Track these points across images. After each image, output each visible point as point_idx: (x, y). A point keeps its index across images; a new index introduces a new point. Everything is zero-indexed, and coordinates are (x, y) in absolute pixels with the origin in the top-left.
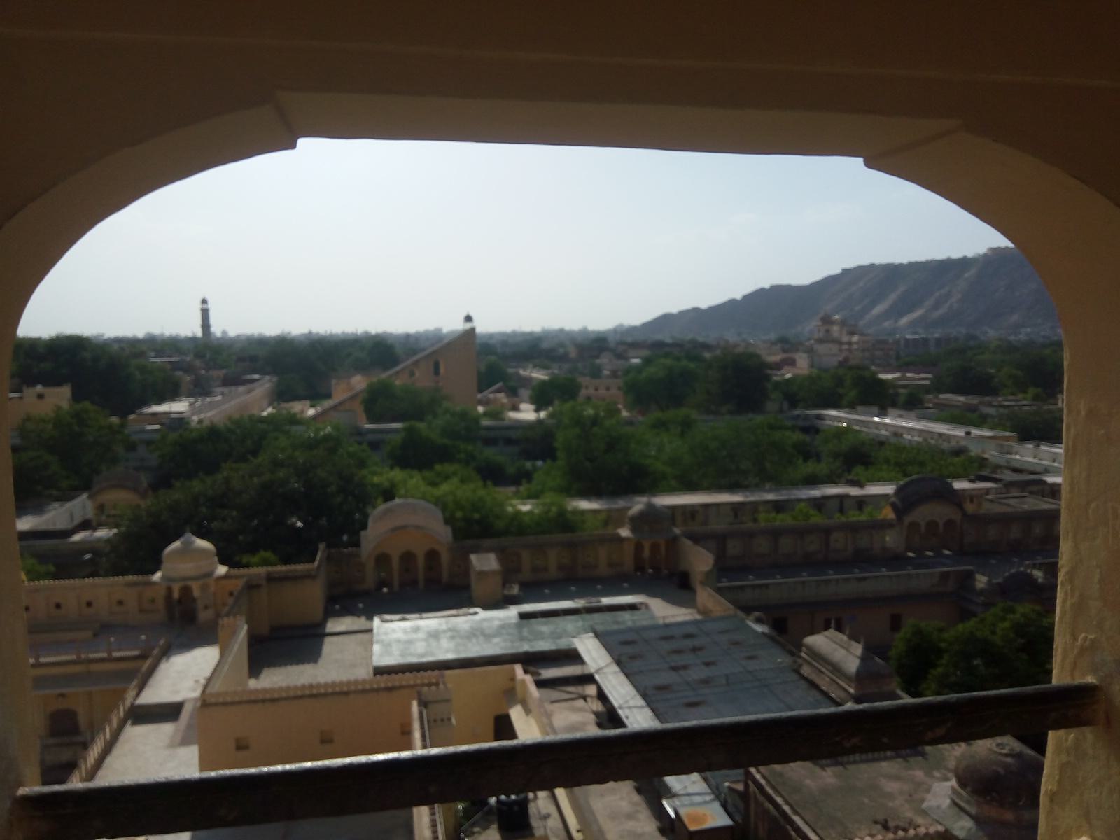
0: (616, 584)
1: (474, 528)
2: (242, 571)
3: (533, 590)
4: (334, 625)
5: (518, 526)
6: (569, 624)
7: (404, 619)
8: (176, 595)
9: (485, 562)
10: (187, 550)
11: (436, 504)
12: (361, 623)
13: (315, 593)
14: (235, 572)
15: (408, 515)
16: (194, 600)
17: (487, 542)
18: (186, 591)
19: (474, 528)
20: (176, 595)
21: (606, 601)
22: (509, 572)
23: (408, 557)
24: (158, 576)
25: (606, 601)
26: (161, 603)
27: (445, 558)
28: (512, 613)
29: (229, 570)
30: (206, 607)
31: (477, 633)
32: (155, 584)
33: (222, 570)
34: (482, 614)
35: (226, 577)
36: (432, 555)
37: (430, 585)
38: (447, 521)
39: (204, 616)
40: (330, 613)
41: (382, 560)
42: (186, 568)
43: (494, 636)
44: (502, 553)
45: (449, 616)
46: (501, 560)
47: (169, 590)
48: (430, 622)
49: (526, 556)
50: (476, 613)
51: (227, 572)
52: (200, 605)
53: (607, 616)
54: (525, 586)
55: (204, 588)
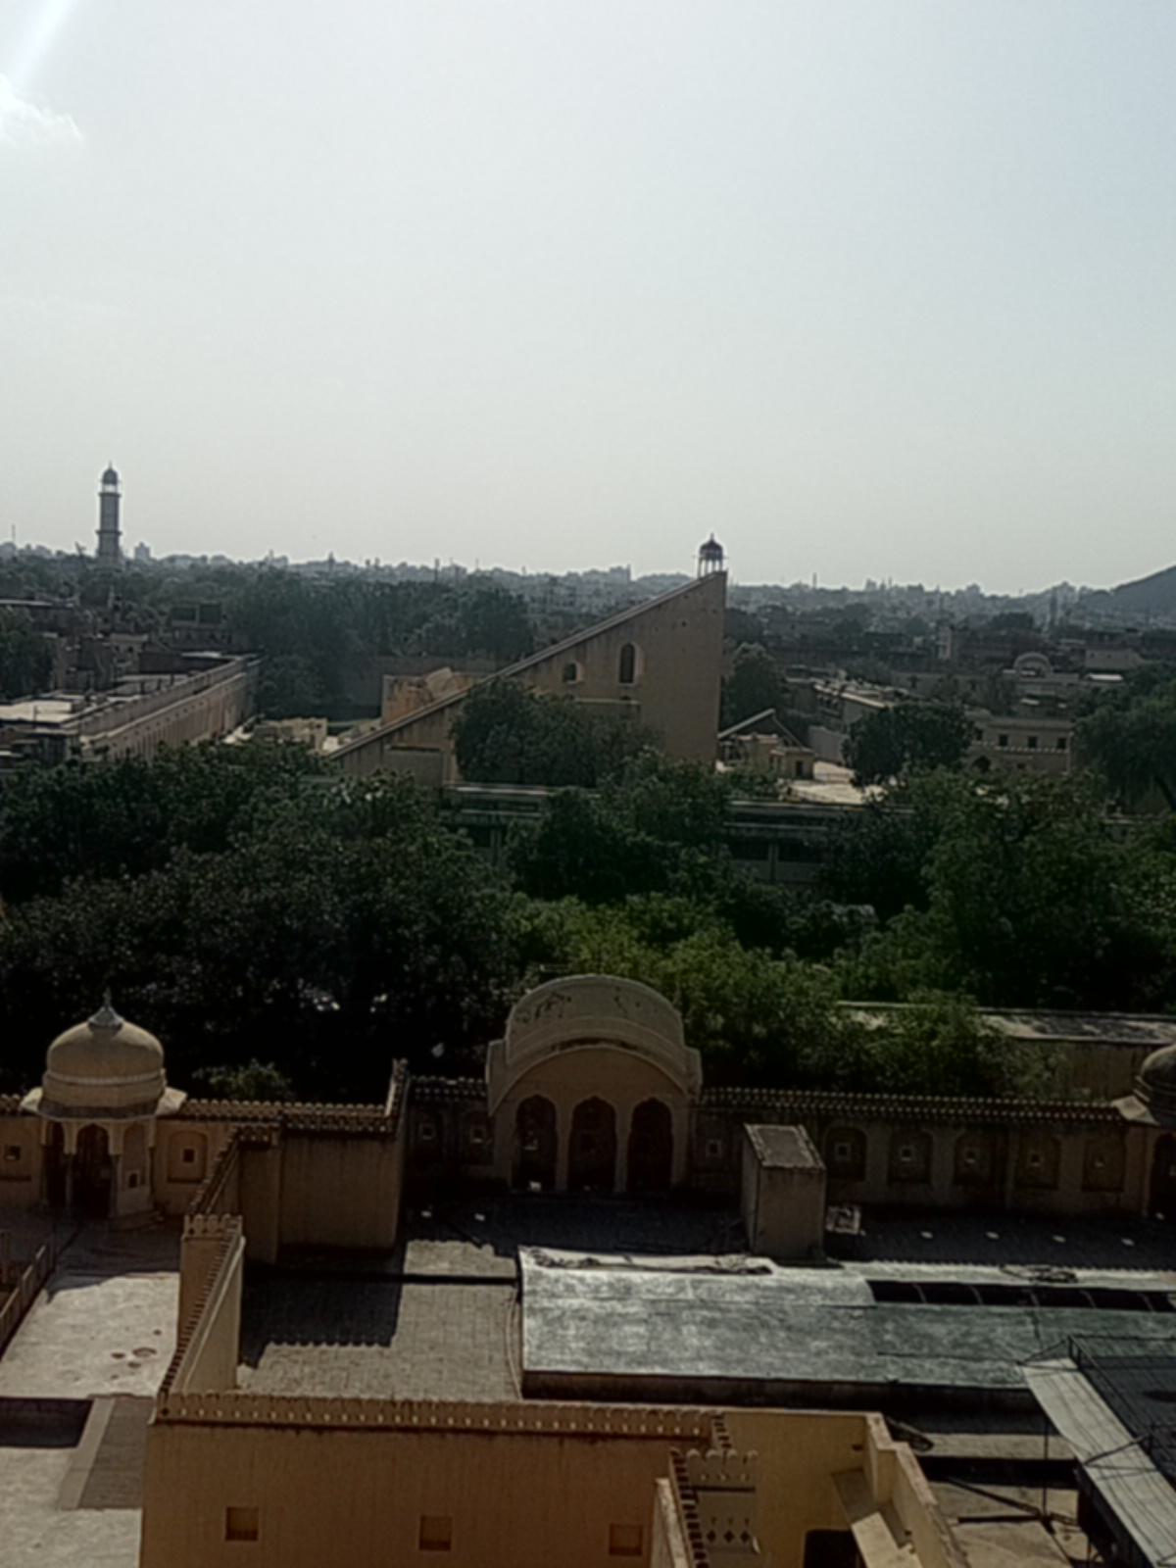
0: (1107, 1231)
1: (755, 1060)
2: (216, 1106)
3: (894, 1225)
4: (421, 1257)
5: (855, 1070)
6: (1001, 1326)
7: (591, 1264)
8: (70, 1147)
9: (783, 1146)
10: (103, 1044)
11: (667, 989)
12: (482, 1259)
13: (382, 1175)
14: (203, 1105)
15: (598, 1016)
16: (108, 1161)
17: (786, 1098)
18: (92, 1138)
19: (755, 1060)
20: (70, 1147)
21: (1087, 1277)
22: (840, 1177)
23: (594, 1115)
24: (36, 1094)
25: (1087, 1277)
26: (35, 1162)
27: (680, 1124)
28: (853, 1278)
29: (188, 1098)
30: (133, 1182)
31: (761, 1319)
32: (26, 1113)
33: (174, 1098)
34: (781, 1275)
35: (178, 1115)
36: (651, 1116)
37: (653, 1192)
38: (695, 1034)
39: (129, 1200)
40: (413, 1228)
41: (535, 1114)
42: (97, 1086)
43: (811, 1332)
44: (822, 1129)
45: (698, 1270)
46: (823, 1142)
47: (57, 1131)
48: (654, 1277)
49: (877, 1142)
50: (765, 1271)
51: (183, 1105)
52: (121, 1174)
53: (1096, 1318)
54: (873, 1215)
55: (134, 1133)
